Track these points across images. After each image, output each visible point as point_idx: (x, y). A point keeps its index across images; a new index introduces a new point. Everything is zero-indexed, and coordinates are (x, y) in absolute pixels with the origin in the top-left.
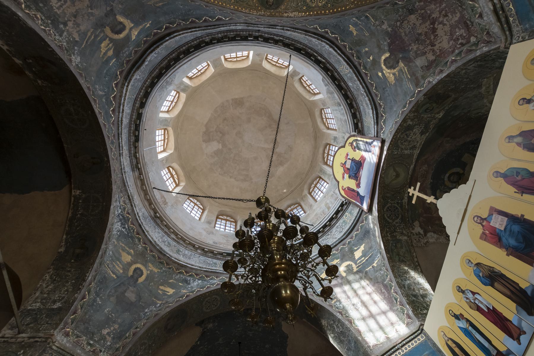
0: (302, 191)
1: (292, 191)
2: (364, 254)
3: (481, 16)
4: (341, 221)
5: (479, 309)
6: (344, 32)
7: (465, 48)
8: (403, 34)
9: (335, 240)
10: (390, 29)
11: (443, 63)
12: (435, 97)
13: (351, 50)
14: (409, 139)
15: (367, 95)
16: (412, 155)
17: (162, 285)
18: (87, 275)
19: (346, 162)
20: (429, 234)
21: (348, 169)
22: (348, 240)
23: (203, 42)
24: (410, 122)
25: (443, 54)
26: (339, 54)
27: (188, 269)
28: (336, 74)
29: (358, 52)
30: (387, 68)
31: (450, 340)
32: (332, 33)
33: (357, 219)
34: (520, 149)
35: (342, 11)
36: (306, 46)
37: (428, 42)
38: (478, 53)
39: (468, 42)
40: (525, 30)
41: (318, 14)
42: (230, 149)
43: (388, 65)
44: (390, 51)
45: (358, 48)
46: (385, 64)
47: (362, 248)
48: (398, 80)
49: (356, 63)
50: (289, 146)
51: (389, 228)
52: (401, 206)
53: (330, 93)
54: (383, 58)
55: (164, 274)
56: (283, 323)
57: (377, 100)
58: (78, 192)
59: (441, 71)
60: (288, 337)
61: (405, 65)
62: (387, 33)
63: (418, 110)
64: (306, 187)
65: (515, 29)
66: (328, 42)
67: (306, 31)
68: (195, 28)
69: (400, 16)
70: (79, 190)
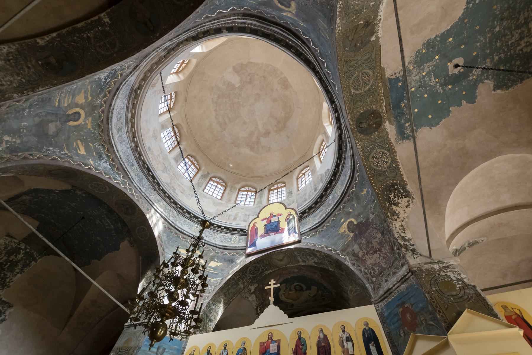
0: (238, 183)
1: (234, 173)
3: (386, 281)
4: (230, 236)
6: (361, 185)
7: (369, 276)
8: (369, 231)
9: (213, 241)
10: (370, 220)
11: (358, 264)
13: (352, 194)
14: (308, 257)
16: (299, 262)
17: (81, 141)
18: (40, 89)
19: (275, 216)
20: (254, 296)
21: (271, 221)
22: (219, 251)
24: (318, 254)
25: (363, 261)
26: (347, 185)
27: (111, 150)
30: (348, 225)
32: (358, 176)
34: (316, 339)
35: (372, 184)
37: (369, 250)
38: (367, 285)
39: (373, 277)
42: (240, 95)
45: (355, 198)
46: (349, 222)
47: (219, 264)
48: (342, 236)
49: (345, 200)
51: (243, 274)
53: (321, 178)
54: (353, 220)
55: (92, 135)
56: (126, 241)
57: (326, 224)
59: (354, 265)
60: (118, 250)
62: (368, 218)
64: (243, 183)
65: (382, 304)
67: (353, 156)
68: (319, 65)
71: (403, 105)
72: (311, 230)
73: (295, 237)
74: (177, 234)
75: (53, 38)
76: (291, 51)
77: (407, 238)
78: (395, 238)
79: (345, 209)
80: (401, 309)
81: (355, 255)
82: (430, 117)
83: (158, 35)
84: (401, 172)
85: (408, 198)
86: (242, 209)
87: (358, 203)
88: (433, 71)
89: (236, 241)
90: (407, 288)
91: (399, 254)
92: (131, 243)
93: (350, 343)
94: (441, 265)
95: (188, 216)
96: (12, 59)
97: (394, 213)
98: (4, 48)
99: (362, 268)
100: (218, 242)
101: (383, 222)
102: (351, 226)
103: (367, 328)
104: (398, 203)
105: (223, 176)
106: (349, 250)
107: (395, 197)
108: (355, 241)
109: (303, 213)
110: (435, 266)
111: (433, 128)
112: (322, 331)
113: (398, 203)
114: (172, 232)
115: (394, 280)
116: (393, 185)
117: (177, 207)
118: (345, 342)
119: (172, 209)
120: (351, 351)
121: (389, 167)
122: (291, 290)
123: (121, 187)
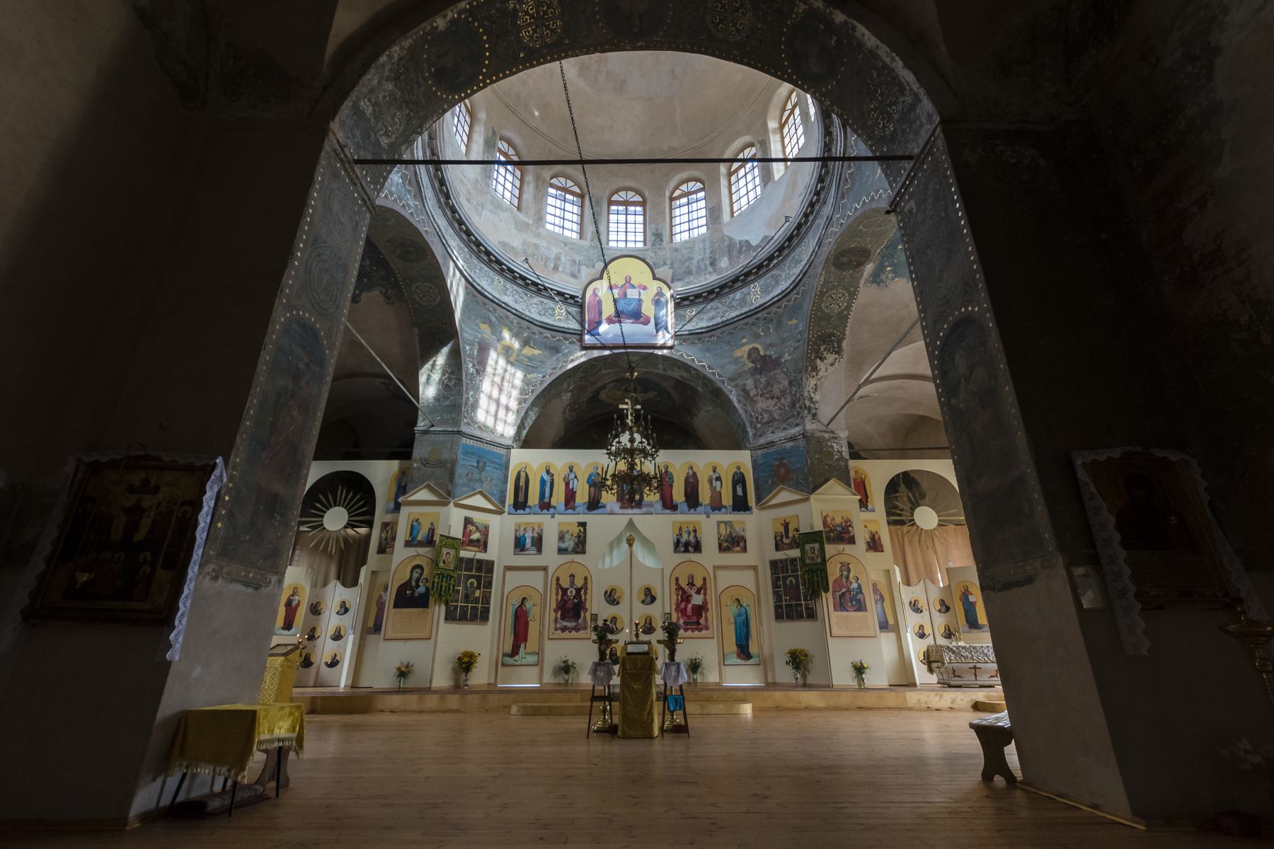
2: (530, 359)
4: (551, 303)
5: (567, 484)
12: (717, 394)
19: (633, 287)
25: (753, 402)
29: (771, 320)
36: (793, 250)
47: (537, 352)
50: (624, 82)
54: (759, 347)
59: (739, 401)
62: (781, 357)
81: (746, 392)
86: (566, 244)
91: (799, 414)
92: (388, 298)
97: (815, 369)
99: (749, 408)
105: (517, 140)
106: (740, 382)
108: (752, 375)
109: (683, 299)
110: (827, 435)
115: (780, 435)
116: (832, 335)
117: (470, 241)
120: (718, 489)
121: (838, 314)
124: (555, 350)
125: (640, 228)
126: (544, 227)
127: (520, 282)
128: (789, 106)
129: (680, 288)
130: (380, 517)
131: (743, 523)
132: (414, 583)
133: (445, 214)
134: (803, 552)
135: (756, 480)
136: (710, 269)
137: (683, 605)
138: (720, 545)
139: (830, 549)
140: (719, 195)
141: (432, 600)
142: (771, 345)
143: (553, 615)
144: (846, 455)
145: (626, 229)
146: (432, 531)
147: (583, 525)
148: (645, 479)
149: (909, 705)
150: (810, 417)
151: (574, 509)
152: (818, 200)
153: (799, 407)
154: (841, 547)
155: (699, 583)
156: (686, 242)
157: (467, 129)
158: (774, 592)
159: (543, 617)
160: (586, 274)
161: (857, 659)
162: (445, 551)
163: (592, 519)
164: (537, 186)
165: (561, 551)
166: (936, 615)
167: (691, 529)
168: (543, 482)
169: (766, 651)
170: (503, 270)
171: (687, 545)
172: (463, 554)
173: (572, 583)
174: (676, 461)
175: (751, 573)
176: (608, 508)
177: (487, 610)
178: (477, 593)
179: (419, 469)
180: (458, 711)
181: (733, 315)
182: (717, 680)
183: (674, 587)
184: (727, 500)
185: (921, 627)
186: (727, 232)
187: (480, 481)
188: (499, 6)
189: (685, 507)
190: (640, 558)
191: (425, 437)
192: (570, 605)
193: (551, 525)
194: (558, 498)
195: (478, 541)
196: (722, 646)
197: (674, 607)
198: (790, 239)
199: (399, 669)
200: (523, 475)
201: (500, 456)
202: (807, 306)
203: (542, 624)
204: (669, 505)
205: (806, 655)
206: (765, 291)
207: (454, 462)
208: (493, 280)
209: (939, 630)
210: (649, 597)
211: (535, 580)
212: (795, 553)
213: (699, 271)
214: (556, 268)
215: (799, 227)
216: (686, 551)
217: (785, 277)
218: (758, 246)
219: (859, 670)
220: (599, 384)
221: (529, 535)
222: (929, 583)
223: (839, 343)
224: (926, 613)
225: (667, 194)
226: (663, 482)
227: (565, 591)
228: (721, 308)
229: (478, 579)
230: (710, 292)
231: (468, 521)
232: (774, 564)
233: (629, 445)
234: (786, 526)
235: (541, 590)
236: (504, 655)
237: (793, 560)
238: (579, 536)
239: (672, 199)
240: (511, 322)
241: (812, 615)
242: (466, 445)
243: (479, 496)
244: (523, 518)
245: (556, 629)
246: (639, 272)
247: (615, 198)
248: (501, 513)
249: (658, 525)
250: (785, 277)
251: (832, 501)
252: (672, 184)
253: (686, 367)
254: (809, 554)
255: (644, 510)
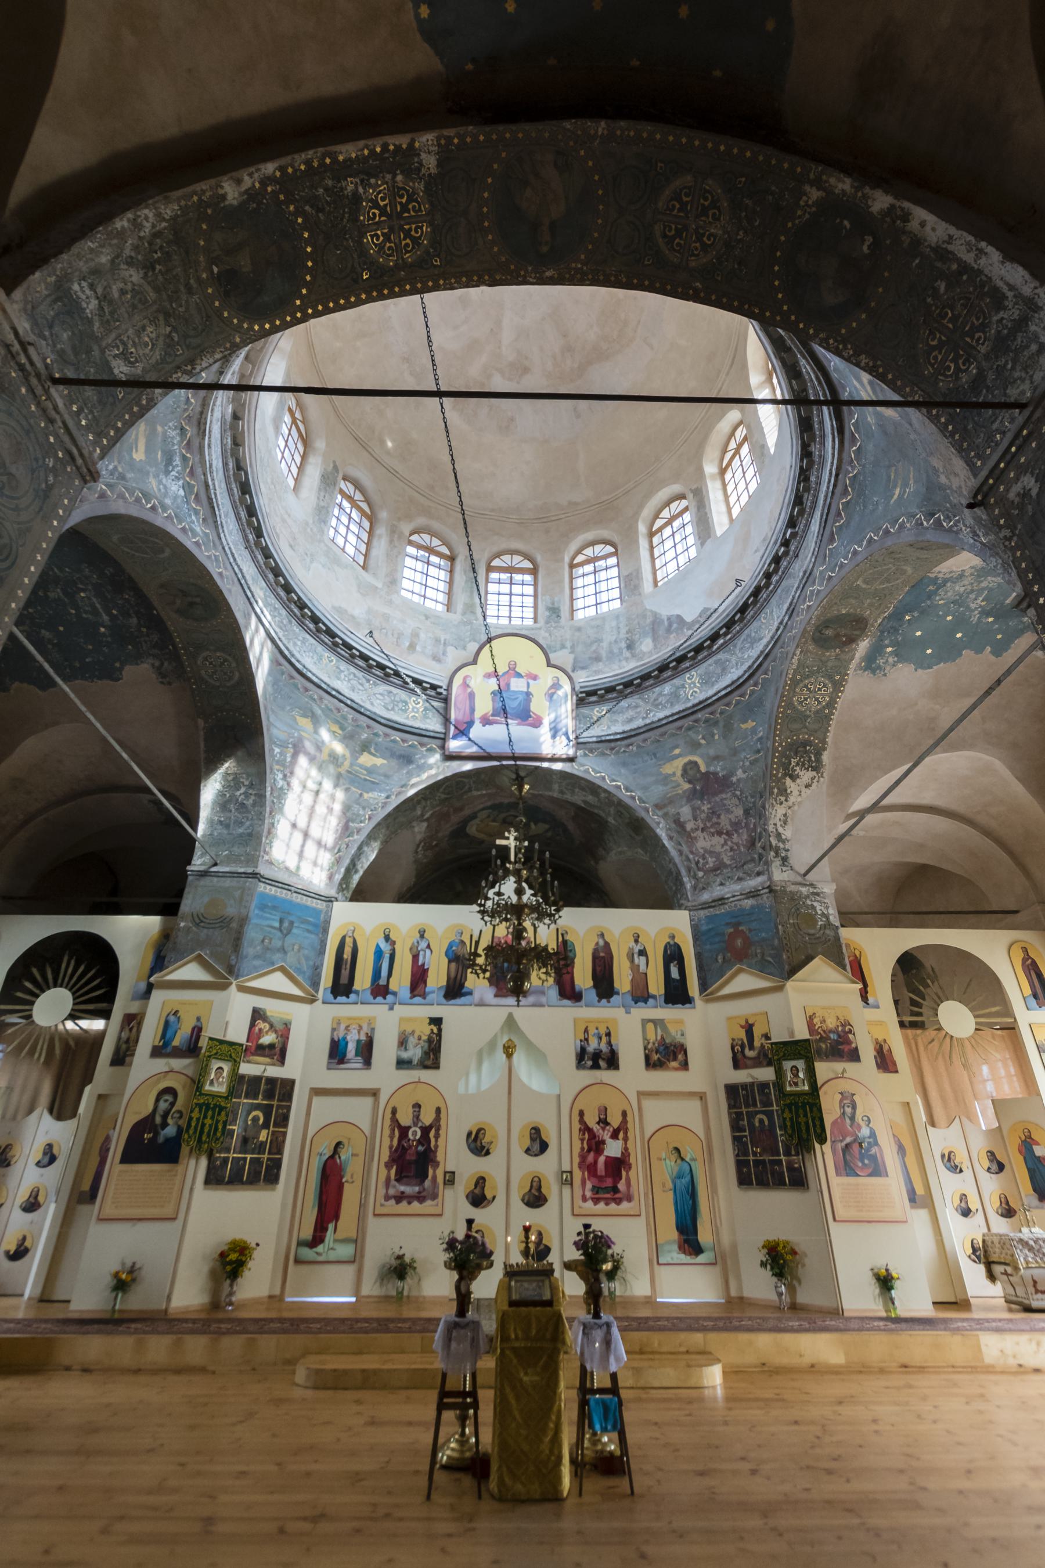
0: (409, 517)
1: (394, 473)
2: (370, 771)
3: (722, 884)
4: (402, 694)
5: (415, 957)
6: (750, 710)
7: (693, 865)
9: (368, 706)
12: (637, 827)
13: (721, 713)
14: (577, 790)
15: (646, 725)
16: (550, 789)
22: (380, 729)
23: (813, 438)
24: (603, 795)
25: (691, 839)
26: (719, 692)
28: (688, 664)
30: (686, 765)
31: (351, 940)
32: (752, 692)
33: (424, 733)
34: (592, 946)
36: (746, 626)
37: (708, 825)
38: (686, 879)
39: (699, 869)
40: (699, 920)
41: (783, 695)
43: (688, 767)
44: (707, 773)
45: (721, 724)
46: (691, 762)
47: (379, 761)
48: (666, 779)
49: (699, 715)
50: (512, 419)
52: (466, 792)
53: (653, 623)
56: (145, 666)
58: (430, 162)
59: (671, 838)
61: (684, 792)
62: (732, 774)
63: (621, 808)
64: (421, 521)
65: (702, 913)
66: (741, 680)
67: (767, 655)
68: (835, 486)
69: (746, 797)
70: (439, 165)
71: (907, 618)
72: (601, 741)
73: (562, 748)
74: (292, 677)
75: (265, 181)
76: (790, 384)
77: (783, 837)
78: (765, 830)
79: (690, 733)
80: (732, 930)
81: (679, 824)
82: (929, 651)
83: (548, 274)
84: (830, 725)
85: (814, 773)
86: (427, 617)
87: (725, 737)
88: (991, 590)
89: (417, 713)
90: (752, 907)
91: (761, 857)
92: (162, 674)
93: (643, 959)
94: (811, 890)
95: (312, 626)
96: (159, 261)
97: (784, 792)
98: (147, 218)
99: (685, 849)
100: (378, 708)
101: (758, 795)
102: (690, 770)
103: (672, 943)
104: (798, 776)
106: (672, 810)
107: (797, 764)
108: (689, 800)
109: (590, 694)
110: (804, 890)
111: (920, 671)
112: (602, 935)
113: (798, 776)
114: (283, 673)
116: (805, 744)
117: (290, 600)
118: (636, 956)
119: (278, 605)
120: (643, 968)
121: (817, 712)
122: (494, 821)
123: (203, 555)
124: (406, 759)
125: (529, 601)
126: (398, 592)
127: (361, 663)
128: (733, 445)
129: (585, 679)
130: (122, 1005)
131: (681, 1022)
132: (158, 1120)
133: (254, 559)
134: (779, 1073)
135: (699, 956)
136: (628, 654)
137: (591, 1158)
138: (647, 1058)
139: (823, 1069)
140: (638, 559)
141: (185, 1150)
142: (717, 758)
143: (384, 1172)
144: (835, 920)
145: (510, 601)
146: (197, 1031)
147: (437, 1022)
148: (540, 955)
149: (988, 1360)
150: (777, 862)
151: (424, 996)
152: (786, 553)
153: (759, 847)
154: (839, 1066)
155: (615, 1121)
156: (592, 619)
157: (298, 459)
158: (735, 1139)
159: (367, 1176)
160: (454, 656)
161: (880, 1264)
162: (215, 1065)
163: (452, 1013)
164: (391, 541)
165: (402, 1064)
166: (985, 1177)
167: (603, 1031)
168: (379, 953)
169: (726, 1240)
170: (336, 644)
171: (596, 1056)
172: (247, 1069)
173: (417, 1118)
174: (581, 925)
175: (696, 1104)
176: (477, 996)
177: (277, 1164)
178: (263, 1135)
179: (188, 930)
180: (202, 1370)
181: (661, 715)
182: (649, 1293)
183: (577, 1126)
184: (656, 986)
185: (963, 1197)
186: (650, 605)
187: (283, 950)
188: (330, 183)
189: (591, 995)
190: (525, 1079)
191: (206, 881)
192: (411, 1156)
193: (390, 1022)
194: (401, 980)
195: (272, 1046)
196: (653, 1229)
197: (577, 1160)
198: (743, 609)
199: (116, 1275)
200: (349, 942)
201: (317, 912)
202: (771, 702)
203: (365, 1187)
204: (569, 993)
205: (794, 1253)
206: (706, 682)
207: (243, 921)
208: (321, 658)
209: (993, 1205)
210: (538, 1144)
211: (359, 1111)
212: (766, 1074)
213: (611, 656)
214: (412, 647)
215: (756, 592)
216: (596, 1066)
217: (735, 663)
218: (694, 622)
219: (885, 1282)
220: (467, 812)
221: (352, 1040)
222: (965, 1120)
223: (818, 754)
224: (968, 1173)
225: (567, 559)
226: (560, 961)
227: (404, 1131)
228: (643, 707)
229: (267, 1110)
230: (628, 684)
231: (257, 1015)
232: (732, 1090)
233: (514, 899)
234: (749, 1029)
235: (367, 1131)
236: (301, 1244)
237: (763, 1086)
238: (430, 1041)
239: (572, 566)
240: (345, 718)
241: (799, 1181)
242: (263, 895)
243: (279, 975)
244: (346, 1010)
245: (387, 1198)
246: (527, 656)
247: (496, 563)
248: (312, 1001)
249: (551, 1022)
250: (735, 663)
251: (815, 995)
252: (573, 547)
253: (592, 788)
254: (789, 1075)
255: (531, 999)
